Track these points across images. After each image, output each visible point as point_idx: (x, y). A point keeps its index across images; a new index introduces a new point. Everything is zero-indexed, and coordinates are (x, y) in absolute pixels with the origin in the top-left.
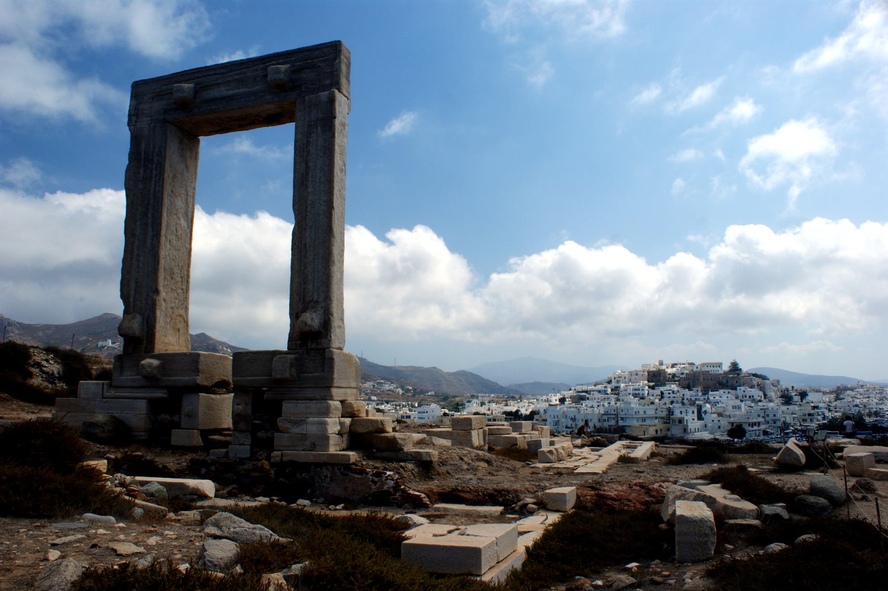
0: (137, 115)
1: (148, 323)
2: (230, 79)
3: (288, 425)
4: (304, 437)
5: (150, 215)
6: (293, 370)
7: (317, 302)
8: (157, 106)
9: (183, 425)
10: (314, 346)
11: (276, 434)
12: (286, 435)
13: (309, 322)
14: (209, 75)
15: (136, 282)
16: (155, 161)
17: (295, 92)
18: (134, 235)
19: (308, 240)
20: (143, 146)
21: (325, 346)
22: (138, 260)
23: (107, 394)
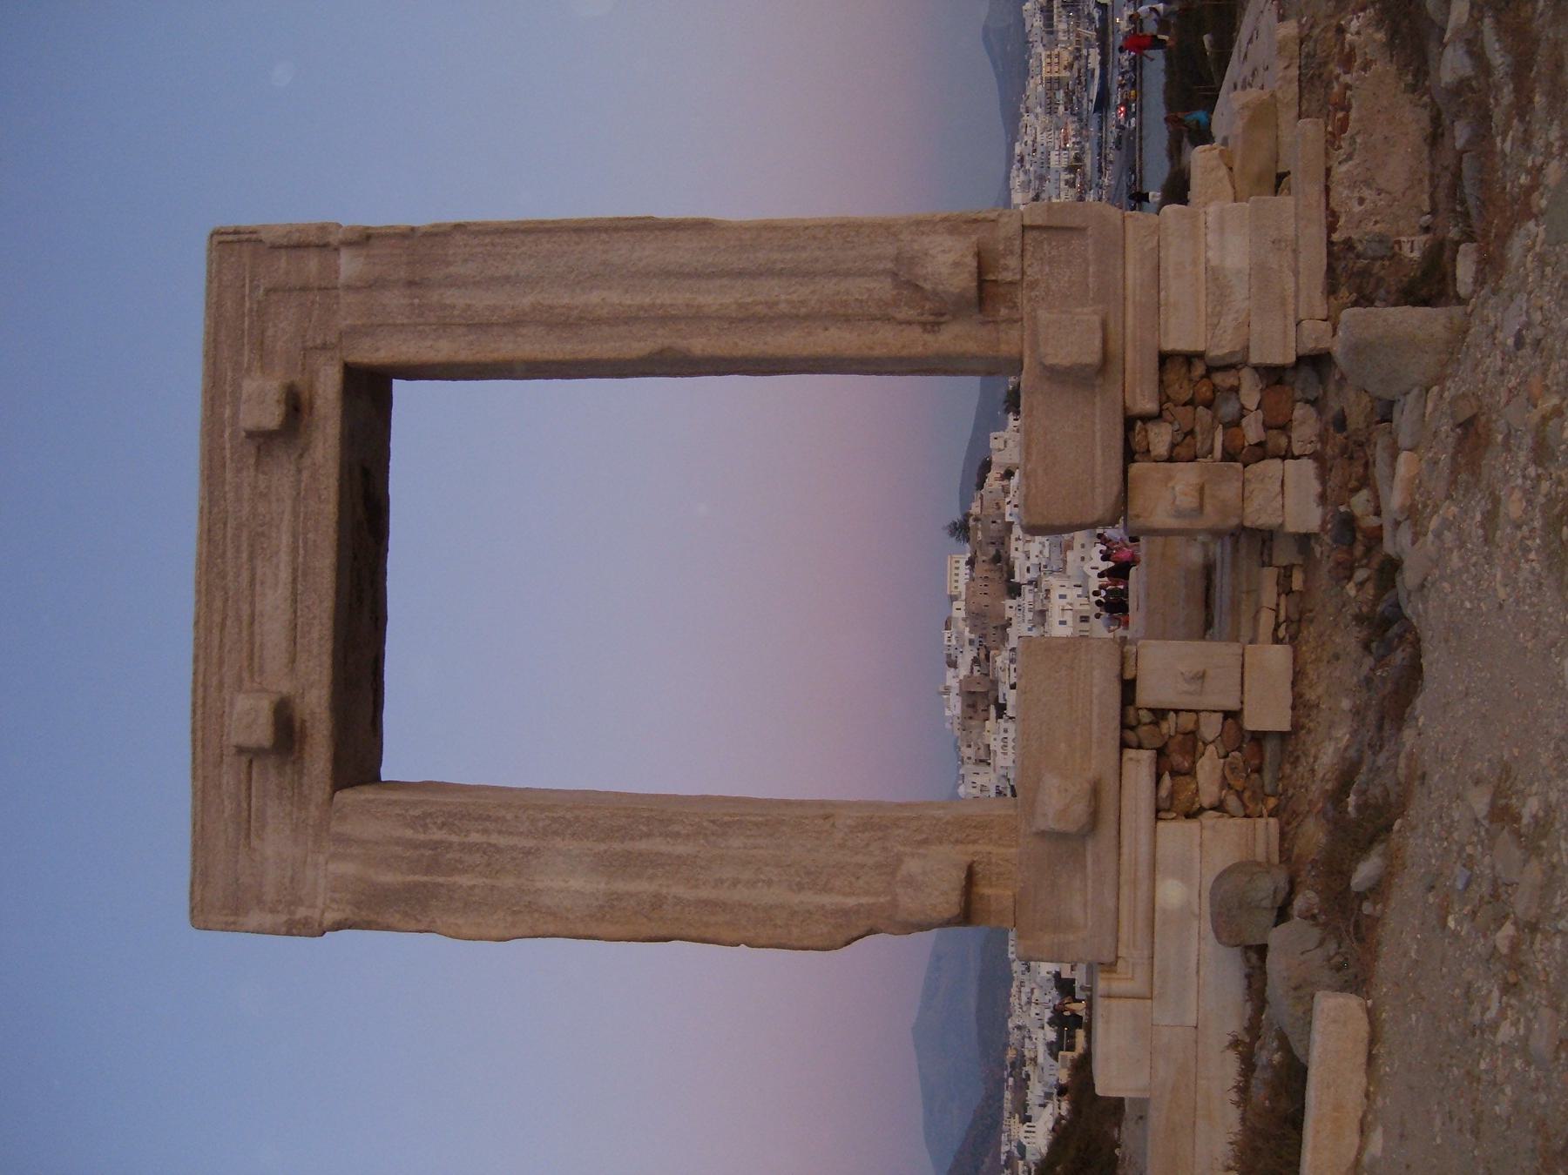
0: (298, 902)
1: (925, 842)
2: (245, 575)
3: (1228, 321)
7: (897, 259)
9: (1231, 704)
10: (1013, 262)
13: (951, 257)
14: (221, 647)
15: (801, 887)
16: (438, 835)
18: (657, 902)
19: (728, 300)
20: (389, 878)
21: (1017, 225)
22: (735, 883)
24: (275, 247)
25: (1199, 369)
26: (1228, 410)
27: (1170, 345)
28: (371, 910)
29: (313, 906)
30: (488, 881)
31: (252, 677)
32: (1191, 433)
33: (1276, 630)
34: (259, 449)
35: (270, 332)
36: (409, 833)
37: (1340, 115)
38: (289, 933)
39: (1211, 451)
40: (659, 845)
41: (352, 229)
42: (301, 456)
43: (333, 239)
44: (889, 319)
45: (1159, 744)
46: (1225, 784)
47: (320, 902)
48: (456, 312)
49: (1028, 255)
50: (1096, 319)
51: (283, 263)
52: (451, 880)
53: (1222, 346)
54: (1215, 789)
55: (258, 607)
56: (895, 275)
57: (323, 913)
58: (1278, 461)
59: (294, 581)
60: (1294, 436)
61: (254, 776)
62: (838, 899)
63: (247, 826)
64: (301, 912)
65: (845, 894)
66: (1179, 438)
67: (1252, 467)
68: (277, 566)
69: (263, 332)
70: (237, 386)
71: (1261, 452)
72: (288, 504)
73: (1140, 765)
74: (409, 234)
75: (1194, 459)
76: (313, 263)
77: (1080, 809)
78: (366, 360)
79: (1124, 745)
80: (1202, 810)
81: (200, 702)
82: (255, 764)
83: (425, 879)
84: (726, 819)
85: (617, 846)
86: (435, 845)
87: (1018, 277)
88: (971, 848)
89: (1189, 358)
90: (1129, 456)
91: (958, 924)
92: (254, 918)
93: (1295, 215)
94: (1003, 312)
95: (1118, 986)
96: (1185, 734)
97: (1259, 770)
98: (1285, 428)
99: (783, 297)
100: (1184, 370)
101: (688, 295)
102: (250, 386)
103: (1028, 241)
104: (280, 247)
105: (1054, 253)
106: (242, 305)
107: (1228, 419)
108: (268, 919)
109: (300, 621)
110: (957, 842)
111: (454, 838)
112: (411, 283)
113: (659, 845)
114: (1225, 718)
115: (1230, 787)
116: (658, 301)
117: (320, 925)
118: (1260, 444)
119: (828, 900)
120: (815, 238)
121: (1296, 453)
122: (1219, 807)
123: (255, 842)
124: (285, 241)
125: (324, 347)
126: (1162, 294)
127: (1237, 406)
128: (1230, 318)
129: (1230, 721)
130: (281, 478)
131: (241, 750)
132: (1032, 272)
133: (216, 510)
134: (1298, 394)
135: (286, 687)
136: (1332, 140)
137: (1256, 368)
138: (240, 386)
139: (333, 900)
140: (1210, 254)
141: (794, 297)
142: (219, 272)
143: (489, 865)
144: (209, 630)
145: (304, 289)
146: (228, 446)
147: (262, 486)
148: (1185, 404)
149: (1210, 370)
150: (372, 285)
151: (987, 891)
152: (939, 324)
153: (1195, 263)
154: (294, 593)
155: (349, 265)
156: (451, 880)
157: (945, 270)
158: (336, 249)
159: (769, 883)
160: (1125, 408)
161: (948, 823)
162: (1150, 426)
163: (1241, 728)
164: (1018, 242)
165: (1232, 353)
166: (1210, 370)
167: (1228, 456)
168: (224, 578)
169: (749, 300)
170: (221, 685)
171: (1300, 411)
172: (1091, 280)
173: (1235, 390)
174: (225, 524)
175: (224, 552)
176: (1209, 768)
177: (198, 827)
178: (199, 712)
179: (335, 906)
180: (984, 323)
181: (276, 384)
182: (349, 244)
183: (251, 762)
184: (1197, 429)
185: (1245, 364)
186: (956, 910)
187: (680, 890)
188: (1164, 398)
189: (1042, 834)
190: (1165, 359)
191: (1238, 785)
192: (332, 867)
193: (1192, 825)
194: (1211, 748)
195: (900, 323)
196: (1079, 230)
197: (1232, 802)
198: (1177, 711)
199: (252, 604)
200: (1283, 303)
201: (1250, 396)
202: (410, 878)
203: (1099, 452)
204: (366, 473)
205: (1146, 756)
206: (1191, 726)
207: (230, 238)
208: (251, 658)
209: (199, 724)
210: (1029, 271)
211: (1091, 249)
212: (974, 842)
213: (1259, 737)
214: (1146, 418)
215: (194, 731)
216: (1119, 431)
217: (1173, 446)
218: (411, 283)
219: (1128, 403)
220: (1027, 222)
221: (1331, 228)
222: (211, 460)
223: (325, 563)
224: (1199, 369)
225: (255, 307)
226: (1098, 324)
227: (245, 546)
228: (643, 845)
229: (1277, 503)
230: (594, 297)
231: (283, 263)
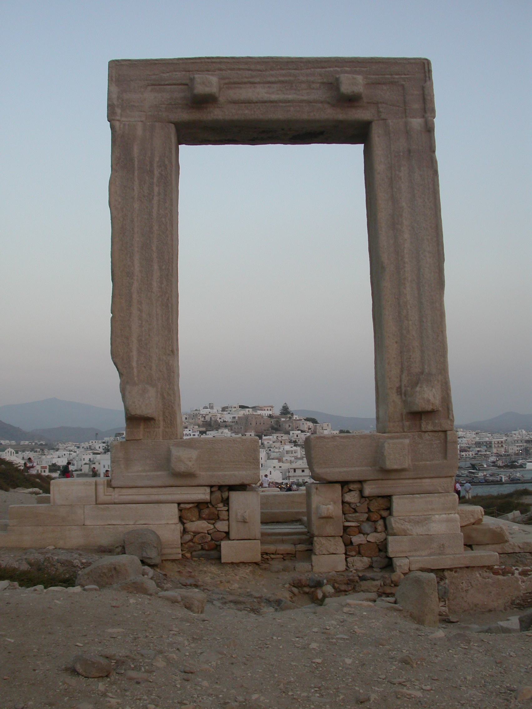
1: (164, 398)
2: (273, 79)
4: (429, 538)
5: (154, 248)
6: (410, 458)
8: (150, 97)
9: (232, 535)
10: (430, 428)
11: (390, 538)
12: (405, 538)
13: (431, 398)
14: (239, 69)
15: (140, 341)
16: (156, 173)
17: (365, 108)
20: (136, 150)
21: (446, 427)
22: (140, 310)
23: (102, 497)
24: (423, 88)
25: (384, 514)
26: (367, 527)
27: (395, 499)
28: (121, 144)
29: (121, 115)
30: (136, 196)
31: (226, 84)
32: (355, 511)
33: (267, 554)
34: (331, 84)
35: (385, 87)
36: (157, 159)
37: (500, 572)
38: (109, 106)
39: (347, 521)
40: (156, 274)
41: (433, 124)
42: (329, 103)
43: (428, 114)
44: (402, 371)
45: (213, 503)
46: (196, 533)
47: (123, 119)
48: (397, 172)
49: (433, 434)
50: (406, 465)
51: (416, 92)
52: (136, 179)
53: (395, 522)
54: (193, 529)
55: (258, 86)
56: (422, 373)
57: (119, 121)
58: (344, 552)
59: (271, 102)
60: (355, 558)
61: (181, 87)
62: (135, 359)
63: (157, 85)
64: (118, 111)
65: (137, 361)
66: (353, 506)
67: (341, 539)
68: (278, 94)
69: (384, 84)
70: (359, 73)
71: (348, 544)
72: (305, 98)
73: (203, 495)
74: (432, 149)
75: (344, 513)
76: (416, 106)
77: (182, 468)
78: (373, 132)
79: (211, 486)
80: (183, 524)
81: (214, 60)
82: (186, 87)
83: (136, 166)
84: (170, 305)
85: (155, 255)
86: (152, 172)
87: (423, 429)
88: (161, 418)
89: (389, 509)
90: (344, 484)
91: (126, 414)
92: (115, 89)
93: (457, 555)
94: (407, 424)
95: (101, 489)
96: (218, 515)
97: (203, 549)
98: (359, 553)
99: (410, 322)
100: (384, 507)
101: (409, 279)
102: (360, 78)
103: (440, 434)
104: (423, 91)
105: (435, 446)
106: (396, 75)
107: (362, 528)
108: (115, 96)
109: (253, 105)
110: (164, 413)
111: (155, 180)
112: (409, 151)
113: (156, 274)
114: (225, 532)
115: (194, 536)
116: (406, 265)
117: (114, 120)
118: (351, 543)
119: (135, 353)
120: (438, 336)
121: (348, 559)
122: (185, 531)
123: (149, 88)
124: (426, 92)
125: (379, 112)
126: (417, 495)
127: (368, 532)
128: (408, 527)
129: (225, 535)
130: (319, 94)
131: (192, 80)
132: (427, 436)
133: (302, 65)
134: (375, 559)
135: (222, 99)
136: (490, 568)
137: (386, 539)
138: (359, 74)
139: (124, 125)
140: (437, 516)
141: (411, 328)
142: (411, 63)
143: (144, 196)
144: (246, 63)
145: (405, 103)
146: (332, 69)
147: (314, 86)
148: (368, 508)
149: (384, 519)
150: (408, 133)
151: (142, 427)
152: (401, 394)
153: (432, 509)
154: (265, 102)
155: (416, 122)
156: (136, 179)
157: (426, 396)
158: (423, 117)
159: (141, 326)
160: (365, 481)
161: (173, 407)
162: (358, 492)
163: (222, 540)
164: (440, 429)
165: (393, 529)
166: (384, 519)
167: (345, 528)
168: (271, 70)
169: (409, 307)
170: (221, 70)
171: (366, 559)
172: (424, 462)
173: (376, 531)
174: (295, 69)
175: (283, 69)
176: (202, 526)
177: (157, 62)
178: (209, 60)
179: (122, 126)
180: (402, 414)
181: (361, 90)
182: (426, 123)
183: (187, 85)
184: (357, 514)
185: (387, 535)
186: (133, 413)
187: (136, 285)
188: (371, 498)
189: (169, 451)
190: (388, 498)
191: (196, 540)
192: (140, 124)
193: (176, 520)
194: (212, 527)
195: (400, 376)
196: (445, 456)
197: (188, 537)
198: (228, 510)
199: (259, 83)
200: (415, 550)
201: (372, 538)
202: (136, 159)
203: (345, 469)
204: (322, 133)
205: (207, 497)
206: (221, 517)
207: (427, 68)
208: (234, 83)
209: (203, 60)
210: (426, 434)
211: (437, 462)
212: (164, 420)
213: (218, 548)
214: (361, 491)
215: (200, 58)
216: (356, 478)
217: (349, 503)
218: (409, 151)
219: (368, 482)
220: (449, 433)
221: (451, 570)
222: (325, 62)
223: (279, 115)
224: (384, 514)
225: (396, 80)
226: (404, 467)
227: (287, 79)
228: (156, 267)
229: (324, 552)
230: (407, 236)
231: (416, 92)
